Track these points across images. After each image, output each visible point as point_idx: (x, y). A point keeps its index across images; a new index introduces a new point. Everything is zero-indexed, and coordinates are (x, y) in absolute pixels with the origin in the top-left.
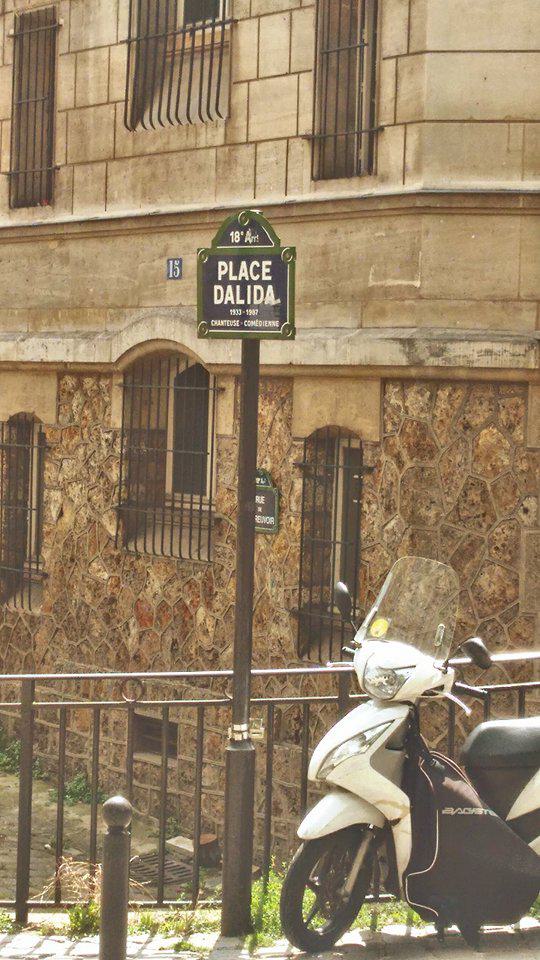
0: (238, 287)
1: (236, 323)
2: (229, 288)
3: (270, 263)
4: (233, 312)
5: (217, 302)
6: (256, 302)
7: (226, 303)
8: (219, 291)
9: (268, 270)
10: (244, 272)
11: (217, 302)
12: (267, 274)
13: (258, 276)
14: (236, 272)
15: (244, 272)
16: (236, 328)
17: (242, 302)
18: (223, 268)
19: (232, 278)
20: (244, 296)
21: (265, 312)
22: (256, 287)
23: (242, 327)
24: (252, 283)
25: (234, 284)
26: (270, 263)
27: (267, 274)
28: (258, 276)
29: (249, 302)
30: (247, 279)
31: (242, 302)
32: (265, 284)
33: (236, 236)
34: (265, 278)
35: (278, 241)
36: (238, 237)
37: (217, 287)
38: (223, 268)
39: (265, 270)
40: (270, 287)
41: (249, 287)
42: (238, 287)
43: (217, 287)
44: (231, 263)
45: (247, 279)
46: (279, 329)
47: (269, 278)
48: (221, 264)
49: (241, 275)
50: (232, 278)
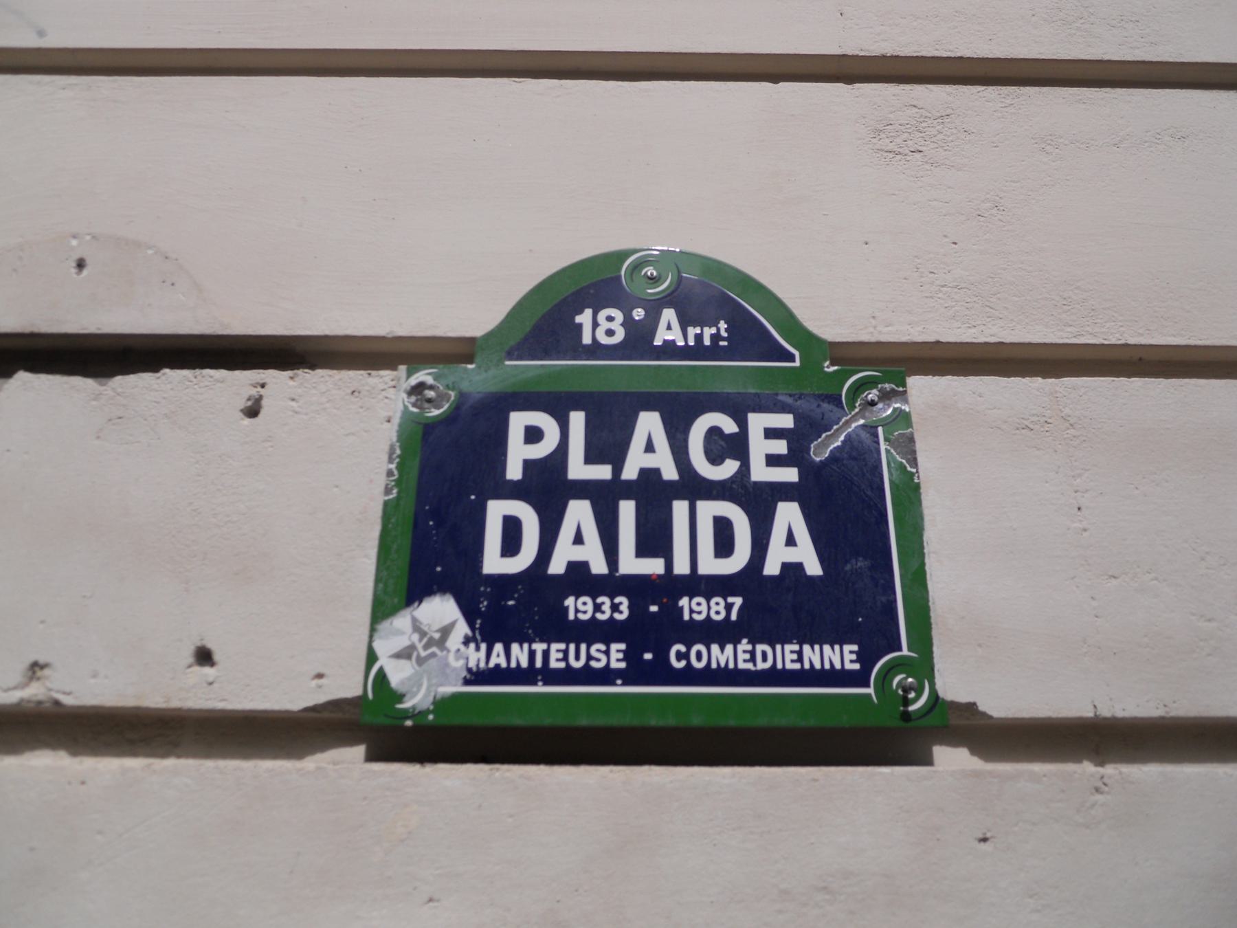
3: (786, 421)
4: (579, 607)
10: (648, 447)
12: (773, 461)
13: (729, 468)
14: (608, 444)
15: (648, 447)
16: (606, 676)
18: (533, 435)
19: (578, 469)
21: (772, 606)
23: (635, 673)
27: (773, 461)
28: (729, 468)
30: (670, 473)
32: (760, 502)
34: (760, 473)
36: (617, 326)
39: (759, 447)
41: (680, 509)
44: (577, 419)
45: (670, 473)
46: (860, 678)
48: (518, 421)
50: (578, 469)
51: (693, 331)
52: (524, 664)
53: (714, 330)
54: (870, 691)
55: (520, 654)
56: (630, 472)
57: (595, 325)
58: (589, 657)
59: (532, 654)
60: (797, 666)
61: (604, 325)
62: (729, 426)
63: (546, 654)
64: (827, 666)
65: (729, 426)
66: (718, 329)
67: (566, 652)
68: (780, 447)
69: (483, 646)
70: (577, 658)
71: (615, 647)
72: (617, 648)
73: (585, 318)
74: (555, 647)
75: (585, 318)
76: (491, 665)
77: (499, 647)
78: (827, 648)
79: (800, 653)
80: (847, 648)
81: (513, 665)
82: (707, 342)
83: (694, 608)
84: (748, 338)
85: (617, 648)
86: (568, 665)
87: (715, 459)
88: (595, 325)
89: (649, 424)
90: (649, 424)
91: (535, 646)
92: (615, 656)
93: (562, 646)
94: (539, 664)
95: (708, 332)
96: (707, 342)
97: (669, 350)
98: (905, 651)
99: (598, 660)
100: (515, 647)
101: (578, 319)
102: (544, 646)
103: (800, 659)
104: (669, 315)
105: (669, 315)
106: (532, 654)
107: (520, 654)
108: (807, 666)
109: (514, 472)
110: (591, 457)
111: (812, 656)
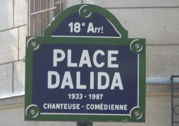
0: (78, 74)
1: (77, 107)
2: (67, 75)
3: (116, 52)
5: (50, 86)
6: (100, 87)
7: (63, 87)
8: (54, 77)
9: (115, 59)
11: (50, 86)
12: (113, 62)
13: (102, 64)
14: (76, 58)
16: (76, 111)
17: (84, 87)
18: (59, 55)
19: (70, 64)
20: (85, 80)
21: (111, 96)
22: (100, 74)
23: (82, 110)
24: (96, 70)
25: (73, 71)
26: (116, 52)
27: (113, 62)
28: (102, 64)
29: (92, 87)
30: (90, 65)
31: (84, 87)
33: (76, 27)
34: (110, 65)
35: (125, 33)
36: (79, 27)
37: (50, 73)
38: (59, 55)
39: (110, 59)
40: (117, 76)
41: (92, 74)
42: (78, 74)
43: (50, 73)
45: (90, 65)
46: (128, 112)
47: (116, 66)
48: (56, 52)
49: (82, 63)
50: (70, 64)
51: (96, 29)
52: (59, 108)
53: (100, 28)
54: (130, 115)
55: (58, 106)
56: (81, 65)
57: (74, 27)
58: (72, 107)
59: (60, 106)
60: (114, 109)
61: (76, 27)
62: (103, 53)
63: (63, 106)
64: (120, 109)
65: (103, 53)
66: (101, 29)
67: (67, 106)
68: (115, 59)
69: (51, 104)
70: (70, 107)
71: (77, 105)
72: (78, 105)
73: (71, 24)
74: (65, 105)
75: (71, 24)
76: (52, 108)
77: (54, 105)
78: (120, 106)
79: (114, 107)
80: (125, 106)
81: (57, 108)
82: (99, 32)
83: (94, 97)
84: (109, 31)
85: (78, 105)
86: (68, 108)
87: (99, 62)
88: (74, 27)
89: (85, 53)
90: (85, 53)
91: (61, 104)
92: (77, 107)
93: (67, 104)
94: (62, 108)
95: (99, 29)
96: (99, 32)
97: (91, 34)
98: (138, 107)
99: (74, 108)
100: (57, 105)
101: (69, 25)
102: (63, 104)
103: (114, 108)
104: (91, 24)
105: (91, 24)
106: (60, 106)
107: (58, 106)
108: (116, 109)
109: (55, 64)
110: (73, 61)
111: (117, 107)
